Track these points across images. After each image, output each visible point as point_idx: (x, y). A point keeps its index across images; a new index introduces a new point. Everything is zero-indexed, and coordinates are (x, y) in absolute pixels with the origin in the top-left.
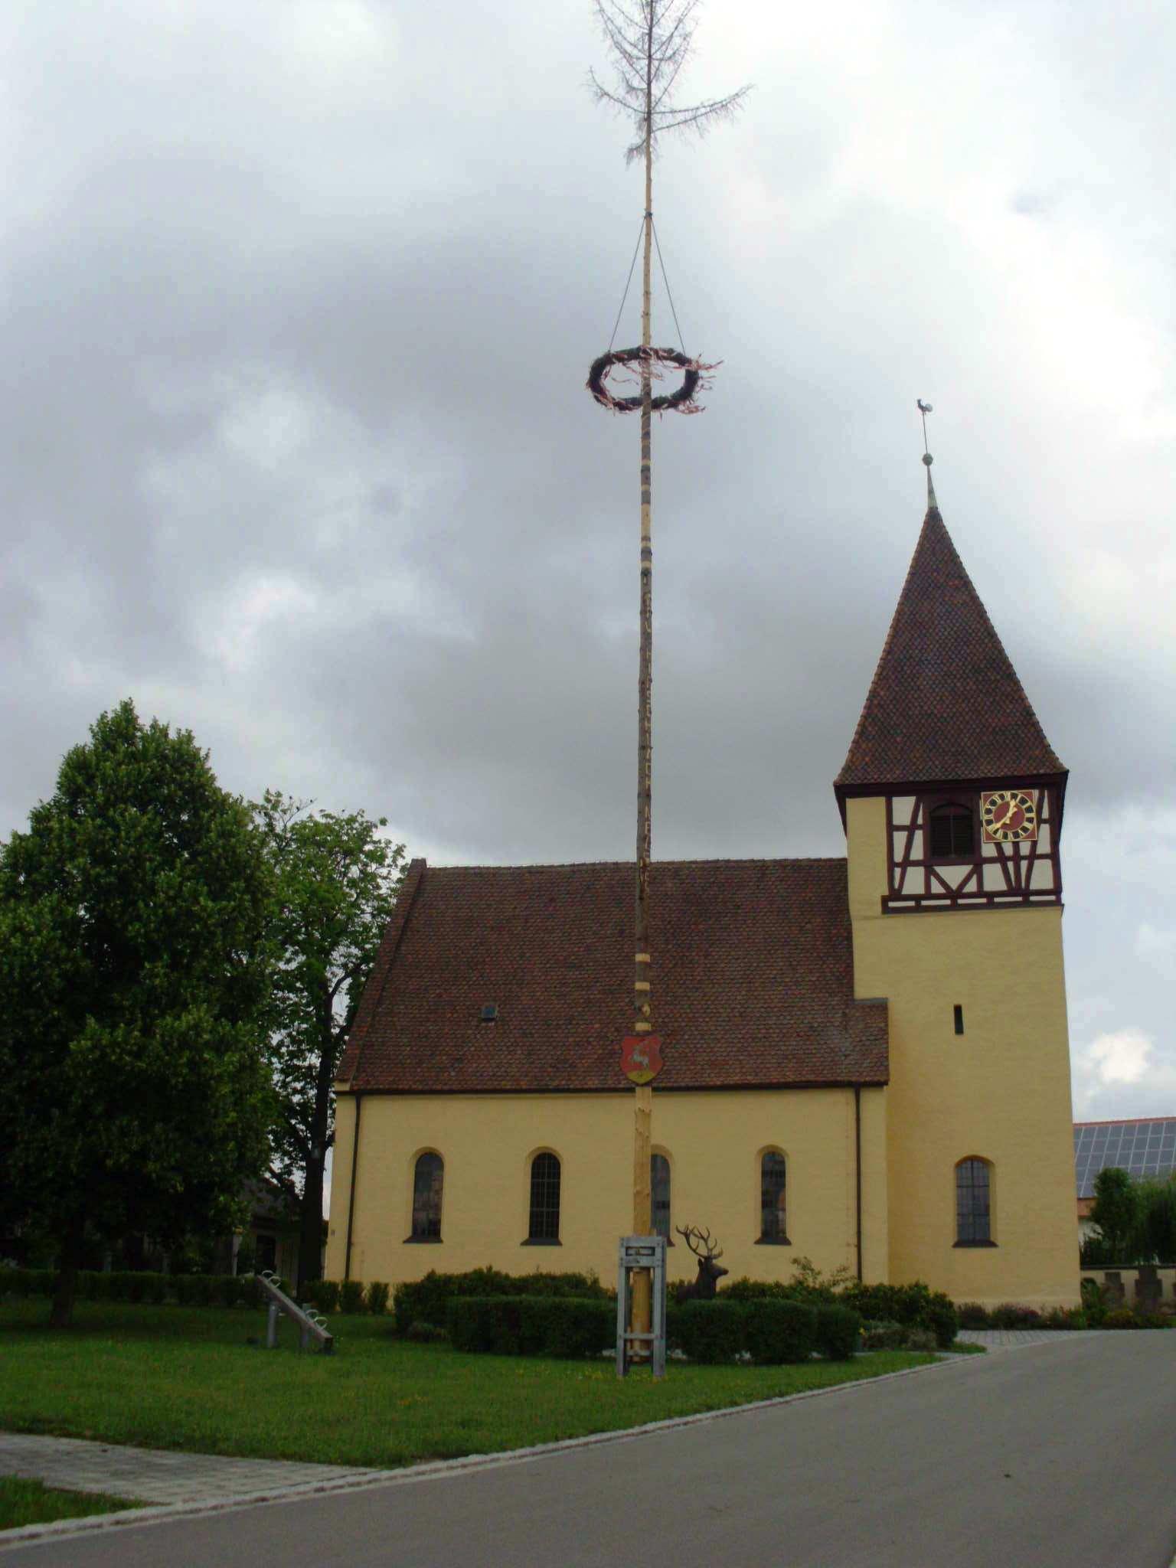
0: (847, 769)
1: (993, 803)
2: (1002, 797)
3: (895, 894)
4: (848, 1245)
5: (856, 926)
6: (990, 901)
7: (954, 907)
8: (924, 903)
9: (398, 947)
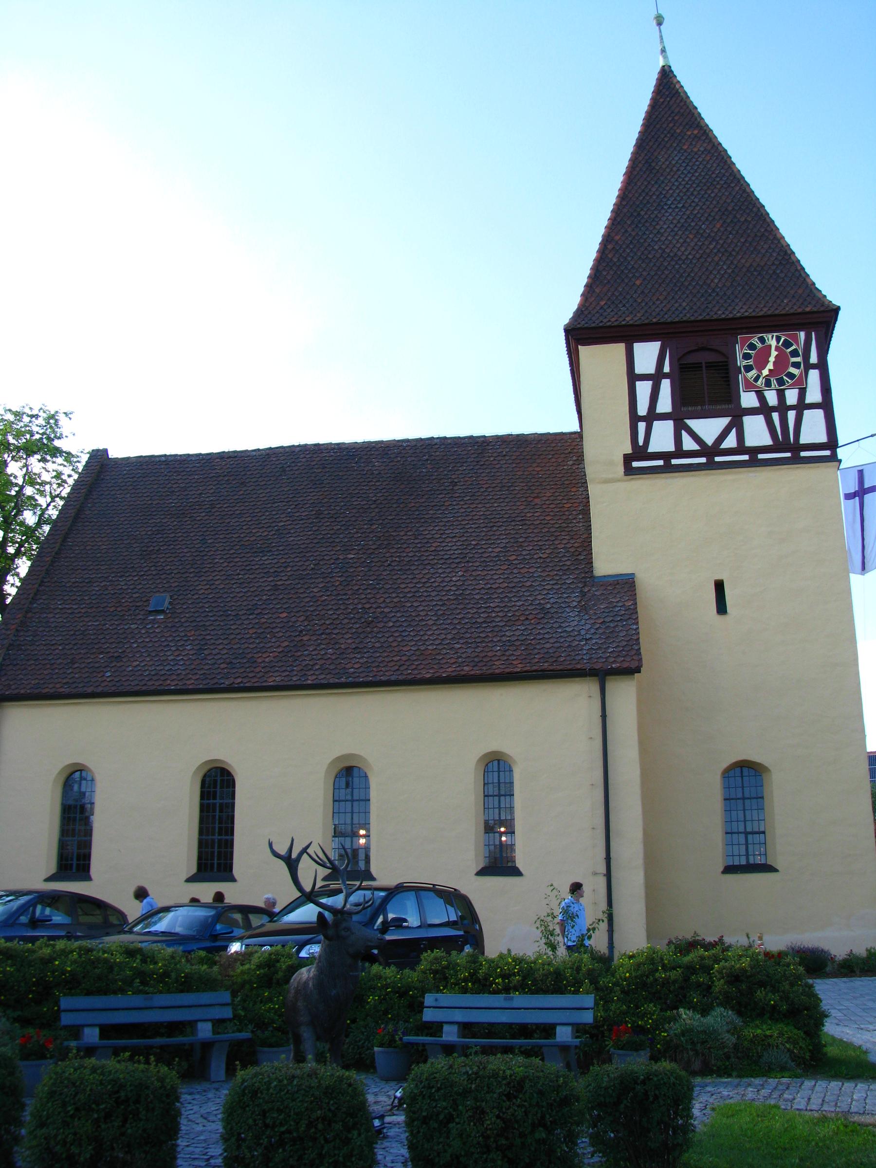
0: (579, 313)
1: (752, 347)
2: (762, 340)
3: (640, 452)
4: (595, 874)
5: (594, 490)
6: (754, 458)
7: (711, 466)
8: (674, 462)
9: (64, 540)
